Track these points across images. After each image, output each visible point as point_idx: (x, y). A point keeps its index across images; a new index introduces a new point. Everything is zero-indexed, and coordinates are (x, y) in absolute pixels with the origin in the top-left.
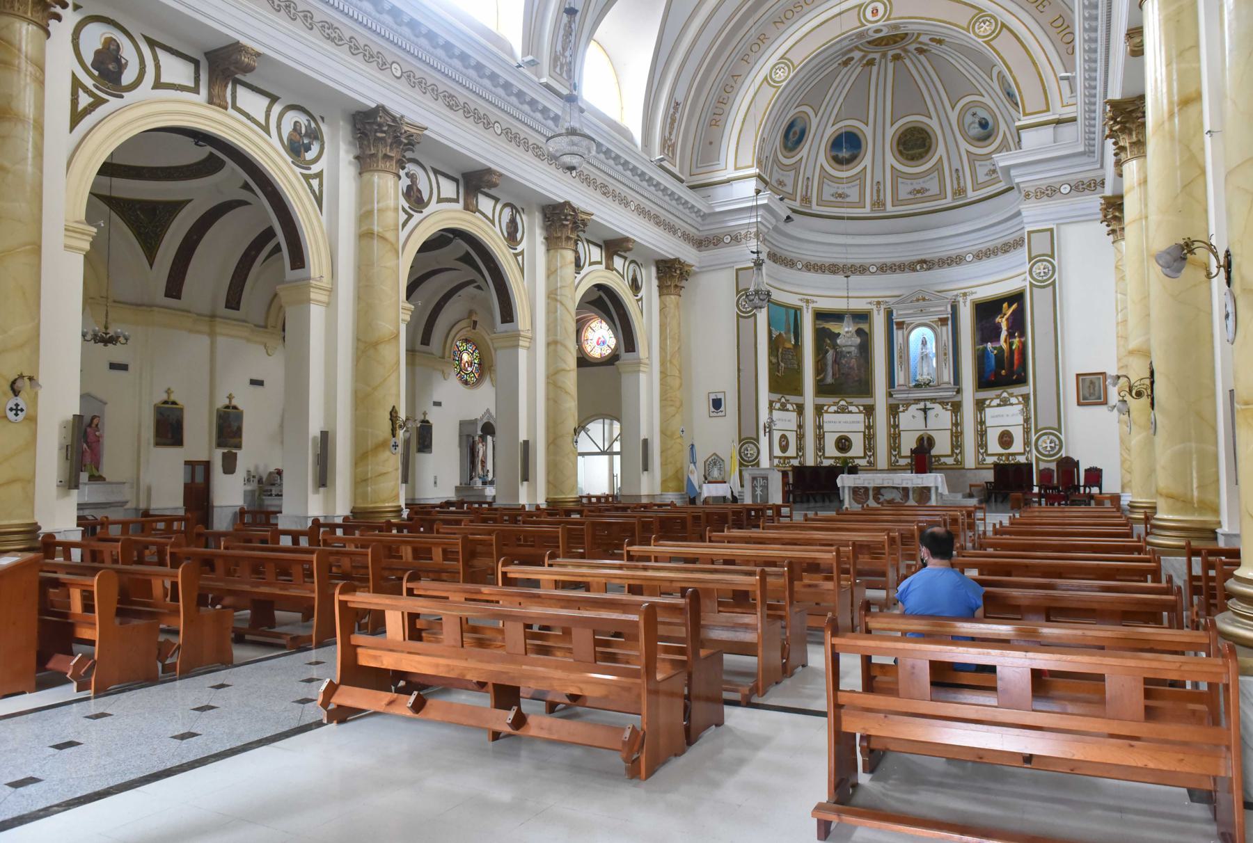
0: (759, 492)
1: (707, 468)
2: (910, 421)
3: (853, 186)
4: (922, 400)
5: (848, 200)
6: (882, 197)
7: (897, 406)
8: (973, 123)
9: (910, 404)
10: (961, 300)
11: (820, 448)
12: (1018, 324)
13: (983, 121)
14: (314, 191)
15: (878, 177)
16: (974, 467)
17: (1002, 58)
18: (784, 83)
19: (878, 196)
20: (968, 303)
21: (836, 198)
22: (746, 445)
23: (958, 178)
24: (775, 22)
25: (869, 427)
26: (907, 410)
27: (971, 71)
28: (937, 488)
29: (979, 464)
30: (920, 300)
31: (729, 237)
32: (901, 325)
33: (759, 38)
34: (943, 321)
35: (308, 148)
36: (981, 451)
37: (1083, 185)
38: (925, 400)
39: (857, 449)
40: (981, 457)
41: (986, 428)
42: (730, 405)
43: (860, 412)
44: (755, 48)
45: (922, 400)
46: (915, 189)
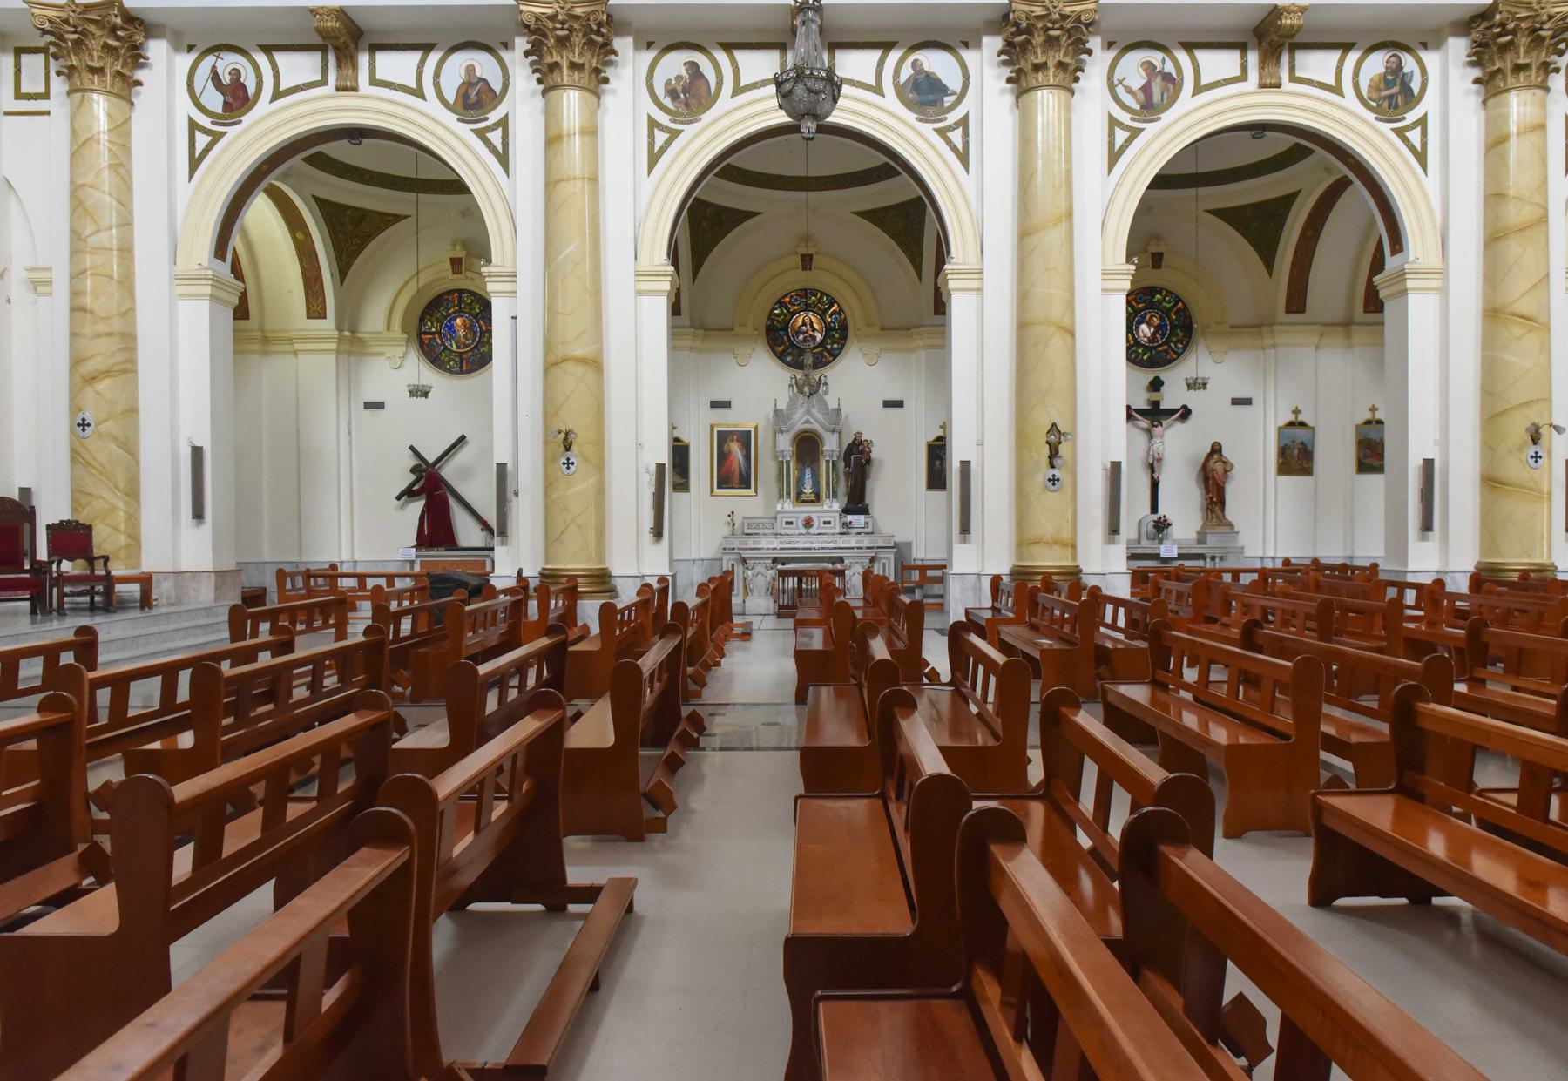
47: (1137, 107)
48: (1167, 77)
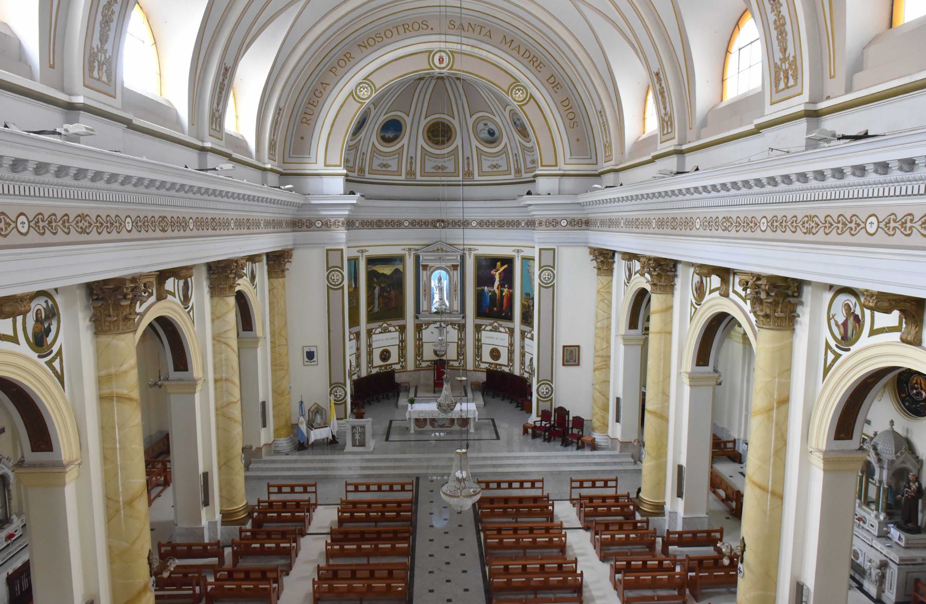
0: (357, 437)
2: (430, 334)
3: (394, 159)
4: (438, 321)
5: (389, 169)
6: (413, 169)
8: (484, 129)
9: (430, 324)
10: (467, 253)
11: (370, 361)
13: (492, 131)
14: (57, 372)
15: (412, 154)
16: (472, 369)
17: (529, 120)
18: (367, 101)
19: (411, 168)
20: (472, 256)
21: (382, 167)
22: (336, 389)
23: (468, 164)
24: (359, 45)
25: (402, 341)
26: (428, 328)
27: (493, 103)
28: (475, 418)
29: (476, 367)
30: (440, 249)
32: (425, 267)
33: (345, 55)
34: (455, 267)
35: (48, 331)
36: (478, 359)
38: (440, 322)
39: (394, 358)
40: (477, 363)
42: (322, 355)
44: (342, 63)
45: (438, 321)
46: (437, 166)
47: (839, 337)
48: (856, 318)
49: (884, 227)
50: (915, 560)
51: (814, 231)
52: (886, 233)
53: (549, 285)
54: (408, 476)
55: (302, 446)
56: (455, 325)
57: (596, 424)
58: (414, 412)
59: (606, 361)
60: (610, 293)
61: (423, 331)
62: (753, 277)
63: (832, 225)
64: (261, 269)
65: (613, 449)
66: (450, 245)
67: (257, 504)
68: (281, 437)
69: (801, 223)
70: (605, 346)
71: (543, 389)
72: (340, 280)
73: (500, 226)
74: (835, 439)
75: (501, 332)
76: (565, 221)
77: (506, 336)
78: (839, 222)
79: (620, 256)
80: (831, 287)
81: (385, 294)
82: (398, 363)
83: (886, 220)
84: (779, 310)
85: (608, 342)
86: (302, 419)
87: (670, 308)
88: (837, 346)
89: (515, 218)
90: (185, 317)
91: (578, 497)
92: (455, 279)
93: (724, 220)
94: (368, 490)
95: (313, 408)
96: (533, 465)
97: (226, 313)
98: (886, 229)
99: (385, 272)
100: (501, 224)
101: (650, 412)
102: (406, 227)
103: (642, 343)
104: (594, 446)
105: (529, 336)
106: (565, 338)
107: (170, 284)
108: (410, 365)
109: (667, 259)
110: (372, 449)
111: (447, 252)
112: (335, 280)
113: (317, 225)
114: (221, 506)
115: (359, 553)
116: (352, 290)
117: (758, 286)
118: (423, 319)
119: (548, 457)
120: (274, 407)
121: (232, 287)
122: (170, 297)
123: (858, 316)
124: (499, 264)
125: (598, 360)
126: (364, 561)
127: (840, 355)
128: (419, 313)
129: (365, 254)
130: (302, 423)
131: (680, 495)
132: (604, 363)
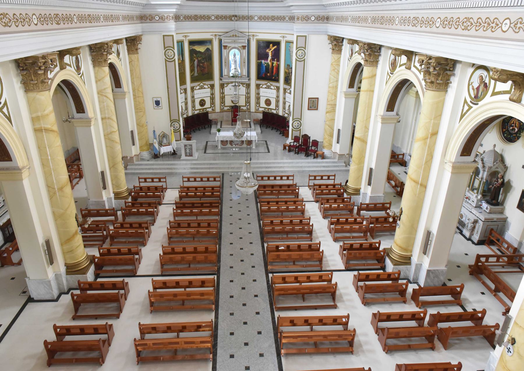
0: (188, 151)
1: (160, 139)
2: (229, 90)
7: (223, 84)
9: (229, 84)
10: (252, 38)
11: (194, 106)
12: (276, 55)
16: (254, 111)
20: (255, 40)
26: (227, 86)
28: (255, 141)
29: (256, 110)
31: (157, 16)
32: (225, 47)
36: (258, 105)
37: (320, 18)
39: (208, 105)
40: (257, 108)
41: (260, 96)
42: (164, 103)
43: (209, 88)
47: (473, 96)
48: (486, 86)
49: (513, 27)
50: (493, 219)
51: (469, 28)
52: (514, 31)
53: (302, 60)
54: (218, 173)
55: (156, 156)
56: (244, 84)
57: (326, 144)
58: (220, 137)
59: (333, 107)
60: (339, 65)
61: (225, 88)
62: (427, 58)
63: (481, 24)
64: (123, 48)
65: (334, 158)
66: (241, 32)
67: (133, 188)
68: (144, 151)
69: (462, 22)
70: (333, 98)
71: (296, 124)
72: (173, 55)
73: (273, 20)
74: (461, 155)
75: (271, 89)
76: (314, 17)
77: (275, 91)
78: (485, 23)
79: (347, 41)
80: (474, 65)
81: (201, 65)
82: (211, 108)
83: (516, 22)
84: (440, 78)
85: (336, 96)
86: (155, 140)
87: (374, 76)
88: (471, 102)
89: (282, 15)
90: (79, 79)
91: (312, 185)
92: (244, 55)
93: (414, 19)
94: (195, 180)
95: (161, 134)
96: (288, 167)
97: (104, 77)
98: (514, 28)
99: (200, 51)
100: (274, 19)
101: (357, 138)
102: (213, 20)
103: (356, 97)
104: (323, 157)
105: (289, 91)
106: (309, 93)
107: (67, 59)
108: (218, 109)
109: (375, 44)
110: (196, 158)
111: (239, 37)
112: (170, 56)
113: (156, 18)
114: (113, 189)
115: (191, 214)
116: (180, 62)
117: (429, 64)
118: (224, 80)
119: (297, 163)
120: (138, 134)
121: (105, 61)
122: (68, 67)
123: (486, 83)
124: (271, 45)
125: (329, 107)
126: (195, 218)
127: (472, 107)
128: (222, 77)
129: (188, 38)
130: (155, 143)
131: (369, 184)
132: (332, 109)
